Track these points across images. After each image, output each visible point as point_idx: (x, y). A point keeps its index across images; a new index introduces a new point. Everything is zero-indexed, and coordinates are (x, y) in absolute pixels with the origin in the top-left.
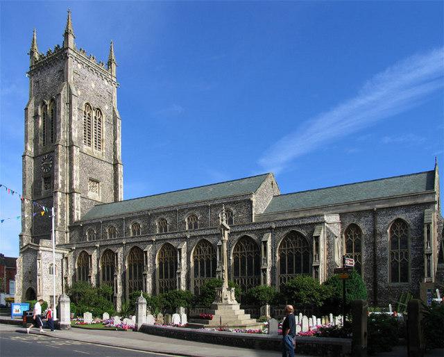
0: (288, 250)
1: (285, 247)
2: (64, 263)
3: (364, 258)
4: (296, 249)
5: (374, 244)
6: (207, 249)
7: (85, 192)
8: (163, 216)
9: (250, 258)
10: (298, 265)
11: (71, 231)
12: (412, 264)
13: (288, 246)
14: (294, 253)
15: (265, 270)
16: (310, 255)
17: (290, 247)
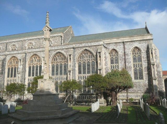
1: (81, 58)
3: (120, 67)
5: (125, 59)
6: (37, 60)
8: (14, 43)
12: (144, 70)
13: (83, 58)
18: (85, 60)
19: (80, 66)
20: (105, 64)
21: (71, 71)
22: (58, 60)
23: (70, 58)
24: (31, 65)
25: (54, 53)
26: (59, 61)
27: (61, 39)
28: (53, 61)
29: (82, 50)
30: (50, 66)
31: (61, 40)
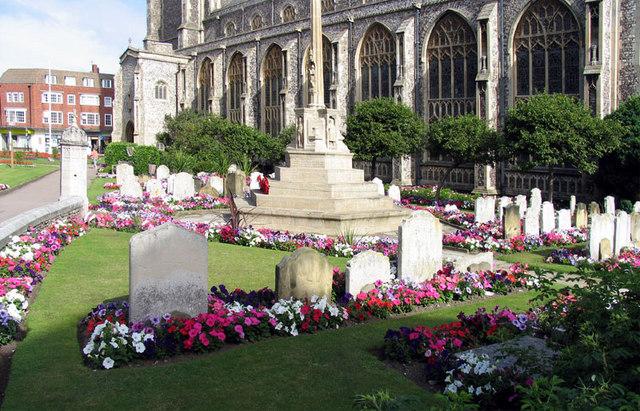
1: (527, 32)
2: (181, 79)
4: (550, 37)
9: (459, 57)
10: (555, 73)
11: (206, 28)
14: (546, 47)
15: (483, 84)
16: (581, 51)
17: (539, 34)
18: (542, 38)
20: (621, 51)
21: (489, 84)
22: (450, 39)
23: (485, 35)
24: (367, 60)
25: (434, 15)
26: (451, 45)
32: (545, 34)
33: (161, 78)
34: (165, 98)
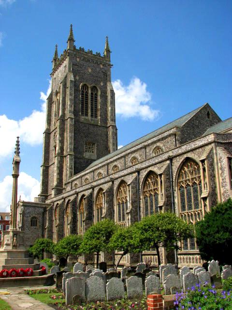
0: (186, 181)
4: (192, 179)
7: (81, 153)
13: (186, 177)
17: (188, 178)
19: (182, 195)
21: (163, 208)
25: (144, 174)
26: (153, 189)
27: (174, 140)
28: (145, 190)
29: (181, 161)
30: (141, 201)
31: (174, 143)
32: (190, 178)
33: (34, 215)
34: (36, 226)
